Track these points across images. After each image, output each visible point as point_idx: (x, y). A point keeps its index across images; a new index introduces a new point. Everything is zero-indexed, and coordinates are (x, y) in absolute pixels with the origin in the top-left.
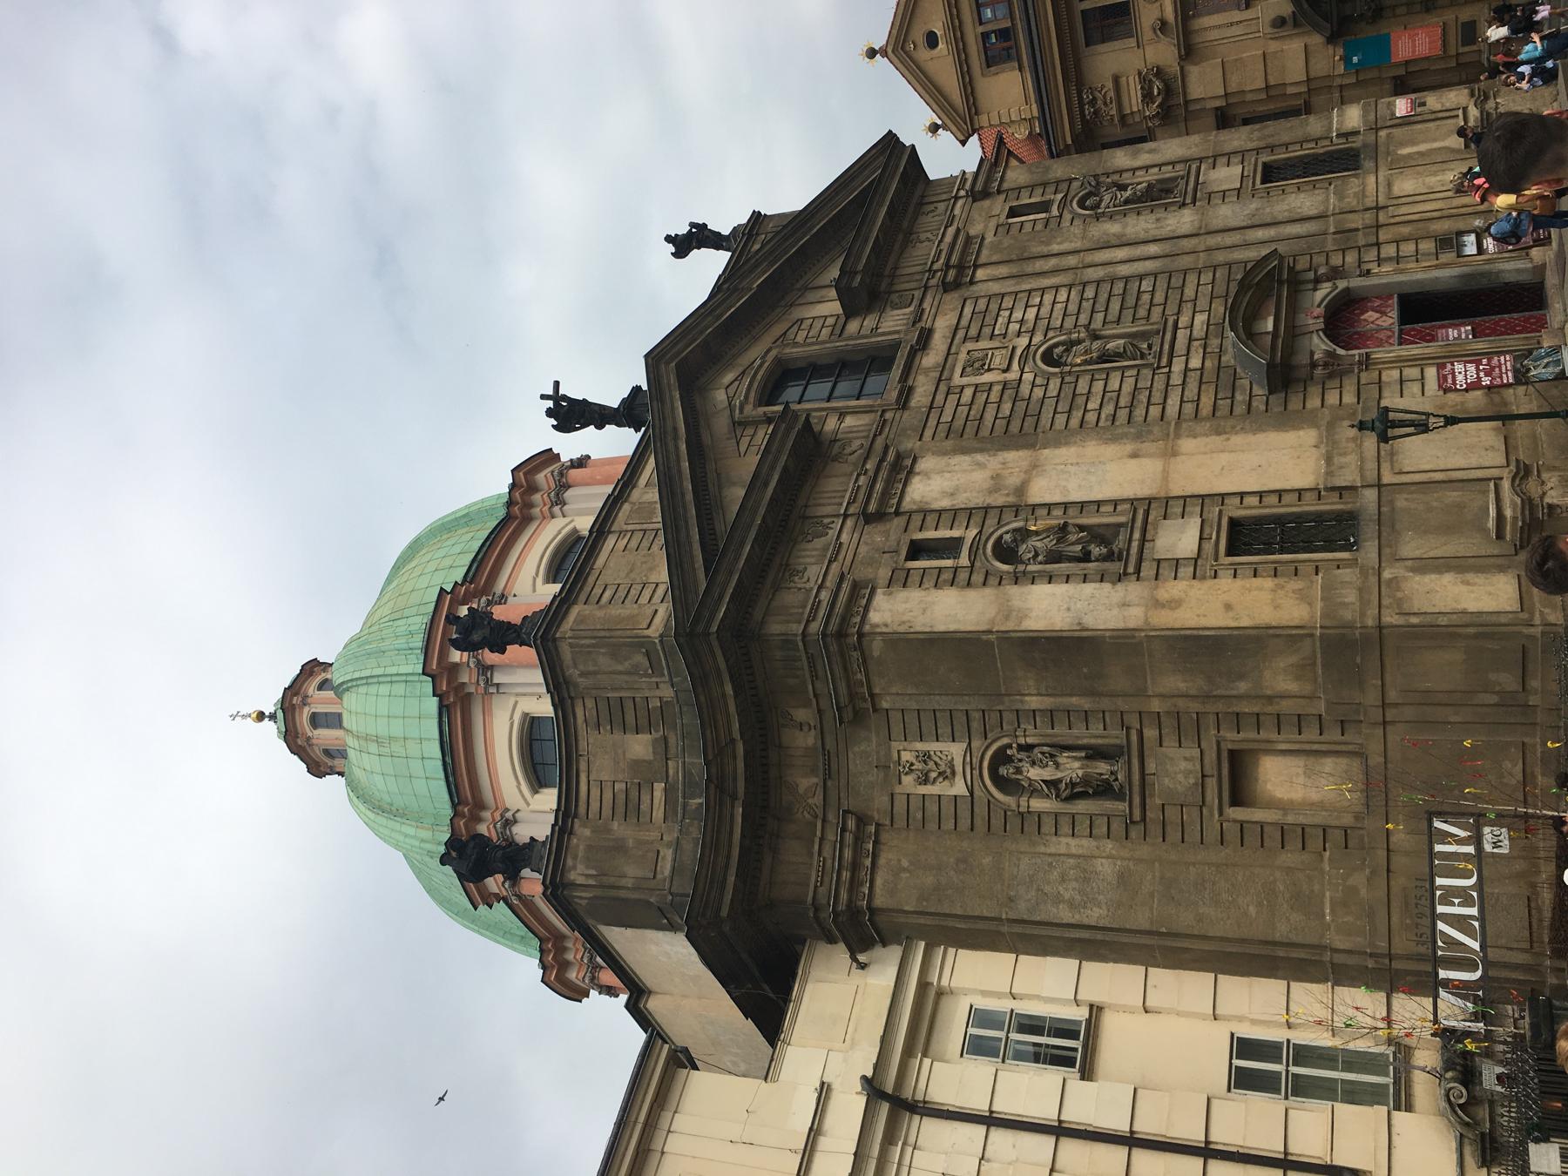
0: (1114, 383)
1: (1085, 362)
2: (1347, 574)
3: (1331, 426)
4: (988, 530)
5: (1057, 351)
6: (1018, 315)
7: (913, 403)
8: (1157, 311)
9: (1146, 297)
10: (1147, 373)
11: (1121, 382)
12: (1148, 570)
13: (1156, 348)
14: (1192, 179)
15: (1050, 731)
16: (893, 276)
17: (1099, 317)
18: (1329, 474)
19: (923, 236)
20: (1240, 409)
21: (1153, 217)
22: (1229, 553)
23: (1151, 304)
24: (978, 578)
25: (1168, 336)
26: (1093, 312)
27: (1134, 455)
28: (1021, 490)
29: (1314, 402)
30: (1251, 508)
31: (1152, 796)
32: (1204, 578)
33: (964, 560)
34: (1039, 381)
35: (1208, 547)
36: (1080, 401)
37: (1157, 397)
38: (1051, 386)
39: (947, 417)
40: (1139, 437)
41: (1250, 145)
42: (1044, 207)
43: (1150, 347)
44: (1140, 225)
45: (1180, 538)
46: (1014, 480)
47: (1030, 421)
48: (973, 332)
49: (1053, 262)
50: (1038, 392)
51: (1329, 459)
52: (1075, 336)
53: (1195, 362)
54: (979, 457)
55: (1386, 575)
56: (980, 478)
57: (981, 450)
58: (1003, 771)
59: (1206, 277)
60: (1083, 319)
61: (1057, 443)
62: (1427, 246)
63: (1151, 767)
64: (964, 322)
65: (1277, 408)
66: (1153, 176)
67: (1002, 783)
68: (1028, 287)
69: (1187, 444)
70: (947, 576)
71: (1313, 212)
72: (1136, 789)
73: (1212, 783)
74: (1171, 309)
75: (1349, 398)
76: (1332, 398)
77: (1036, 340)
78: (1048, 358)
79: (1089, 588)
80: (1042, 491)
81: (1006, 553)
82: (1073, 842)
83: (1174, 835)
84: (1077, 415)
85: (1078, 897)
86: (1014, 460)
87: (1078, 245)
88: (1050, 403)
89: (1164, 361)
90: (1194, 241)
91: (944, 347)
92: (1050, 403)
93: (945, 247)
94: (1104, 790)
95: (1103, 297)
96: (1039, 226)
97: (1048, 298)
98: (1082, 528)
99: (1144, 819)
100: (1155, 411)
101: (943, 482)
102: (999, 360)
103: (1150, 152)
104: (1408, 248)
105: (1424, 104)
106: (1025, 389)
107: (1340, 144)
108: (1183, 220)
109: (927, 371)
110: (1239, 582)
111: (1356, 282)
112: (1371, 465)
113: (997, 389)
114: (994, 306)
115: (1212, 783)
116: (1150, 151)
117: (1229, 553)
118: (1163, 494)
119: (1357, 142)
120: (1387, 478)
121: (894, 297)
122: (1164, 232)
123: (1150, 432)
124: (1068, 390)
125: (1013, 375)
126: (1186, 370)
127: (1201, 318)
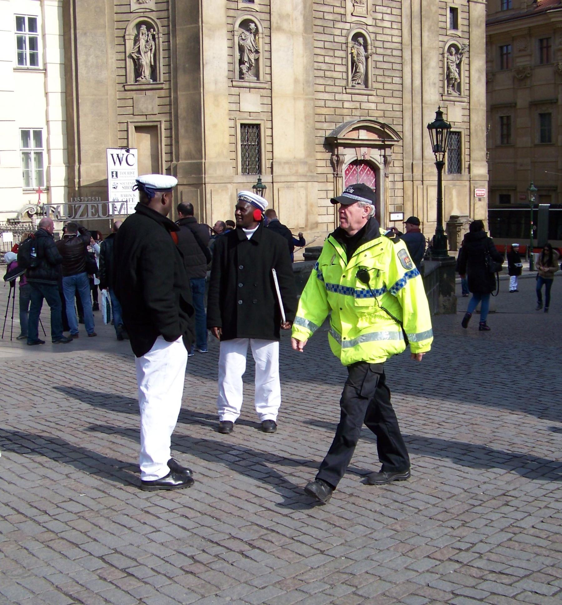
0: (338, 68)
1: (352, 53)
2: (231, 171)
3: (305, 163)
4: (259, 16)
5: (361, 40)
6: (386, 17)
8: (380, 86)
9: (389, 80)
10: (344, 83)
11: (341, 71)
12: (235, 91)
13: (357, 86)
14: (458, 99)
15: (161, 49)
17: (381, 58)
18: (280, 163)
20: (318, 125)
21: (437, 81)
22: (242, 125)
24: (232, 13)
25: (365, 92)
26: (384, 55)
27: (296, 81)
28: (279, 29)
29: (319, 156)
30: (265, 132)
31: (137, 94)
32: (229, 115)
35: (246, 115)
36: (331, 53)
37: (328, 89)
38: (340, 38)
40: (307, 82)
42: (455, 26)
43: (358, 84)
44: (434, 75)
45: (251, 103)
46: (285, 25)
47: (321, 29)
49: (416, 32)
50: (338, 32)
51: (287, 163)
52: (369, 47)
54: (300, 7)
55: (229, 185)
56: (288, 8)
57: (305, 7)
58: (144, 28)
59: (396, 108)
60: (379, 51)
61: (306, 44)
62: (399, 201)
63: (148, 93)
65: (317, 141)
66: (464, 80)
67: (138, 26)
69: (300, 104)
72: (139, 87)
73: (143, 119)
74: (380, 92)
75: (320, 170)
76: (323, 163)
77: (371, 29)
78: (357, 36)
79: (225, 67)
80: (278, 39)
81: (245, 24)
82: (114, 60)
83: (122, 103)
84: (322, 52)
85: (90, 64)
86: (298, 23)
88: (331, 38)
89: (348, 91)
92: (331, 38)
94: (138, 73)
96: (442, 25)
98: (257, 60)
99: (125, 90)
100: (321, 88)
103: (479, 77)
104: (399, 193)
105: (480, 200)
106: (340, 25)
107: (465, 165)
110: (227, 129)
111: (382, 173)
112: (283, 179)
113: (342, 11)
114: (394, 4)
115: (143, 119)
116: (479, 80)
117: (242, 125)
119: (465, 172)
122: (426, 87)
123: (309, 86)
124: (338, 46)
125: (349, 18)
126: (343, 101)
127: (373, 106)
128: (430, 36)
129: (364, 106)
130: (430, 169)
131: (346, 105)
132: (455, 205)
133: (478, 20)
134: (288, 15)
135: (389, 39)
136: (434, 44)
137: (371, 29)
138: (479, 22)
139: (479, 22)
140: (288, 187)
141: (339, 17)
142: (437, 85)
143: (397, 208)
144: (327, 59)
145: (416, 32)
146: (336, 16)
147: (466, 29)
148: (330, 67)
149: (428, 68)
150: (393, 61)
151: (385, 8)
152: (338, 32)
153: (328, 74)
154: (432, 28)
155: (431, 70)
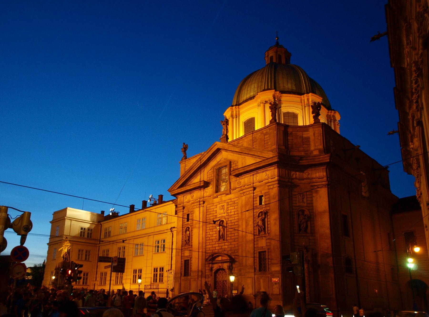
6: (232, 211)
7: (214, 199)
8: (230, 238)
19: (258, 178)
23: (231, 237)
28: (195, 227)
36: (212, 231)
45: (187, 253)
48: (230, 203)
59: (236, 245)
64: (232, 200)
105: (276, 284)
108: (250, 237)
109: (221, 199)
113: (216, 214)
114: (236, 204)
116: (275, 224)
117: (185, 261)
120: (192, 280)
121: (241, 181)
125: (218, 216)
126: (215, 247)
127: (226, 247)
129: (223, 247)
131: (217, 248)
135: (233, 218)
140: (194, 280)
144: (211, 233)
153: (211, 238)
155: (249, 226)
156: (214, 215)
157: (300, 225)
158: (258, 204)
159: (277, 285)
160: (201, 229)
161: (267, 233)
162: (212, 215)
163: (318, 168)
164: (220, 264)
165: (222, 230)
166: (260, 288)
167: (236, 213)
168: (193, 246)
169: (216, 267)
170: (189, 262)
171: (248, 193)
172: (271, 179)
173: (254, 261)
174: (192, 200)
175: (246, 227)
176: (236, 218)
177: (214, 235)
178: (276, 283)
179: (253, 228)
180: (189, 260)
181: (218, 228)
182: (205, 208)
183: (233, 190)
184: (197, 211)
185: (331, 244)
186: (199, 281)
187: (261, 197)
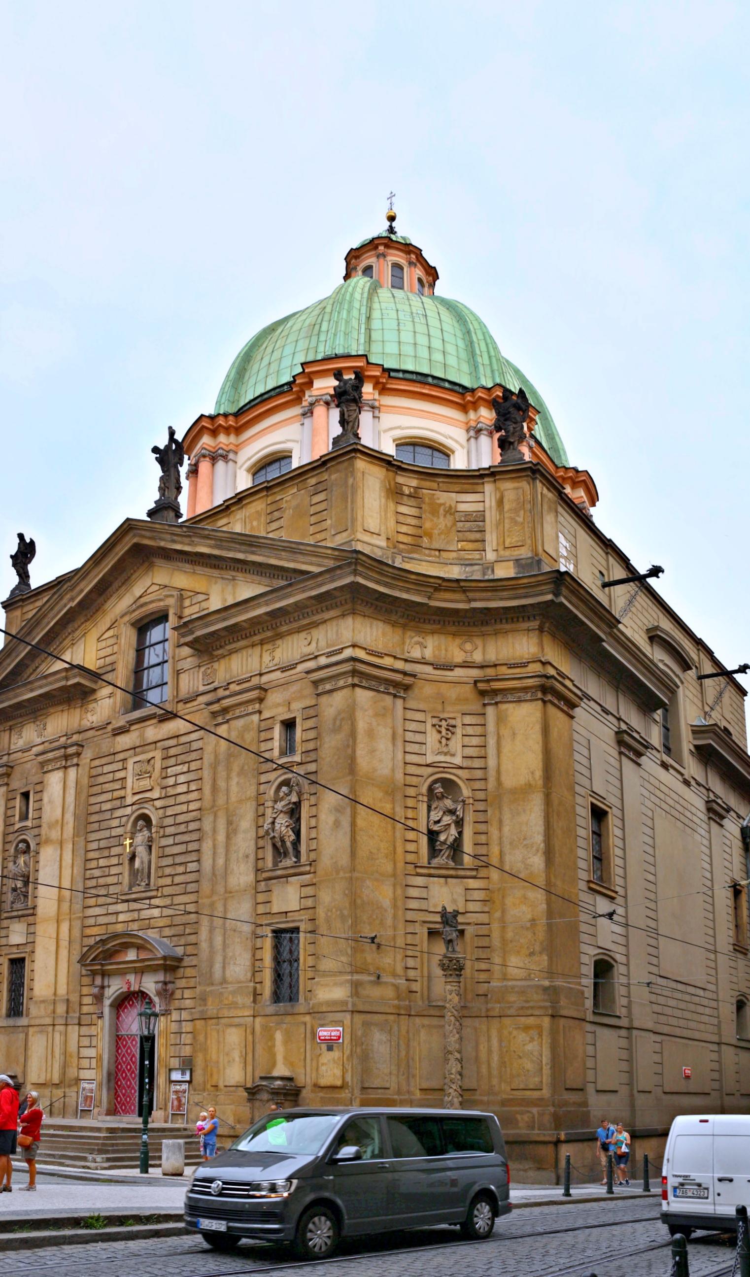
6: (182, 779)
8: (168, 881)
14: (292, 871)
16: (231, 653)
18: (36, 1002)
19: (278, 654)
23: (173, 876)
28: (48, 841)
33: (17, 826)
34: (124, 819)
39: (106, 769)
41: (321, 913)
48: (172, 752)
53: (122, 917)
62: (187, 1051)
68: (206, 774)
69: (65, 927)
70: (12, 820)
71: (228, 973)
75: (85, 1009)
77: (158, 804)
87: (233, 798)
88: (106, 834)
90: (222, 890)
91: (160, 737)
92: (106, 834)
93: (255, 681)
95: (186, 838)
97: (194, 796)
101: (58, 792)
102: (145, 783)
104: (187, 1039)
108: (242, 875)
109: (142, 736)
114: (194, 756)
116: (337, 824)
118: (38, 920)
119: (301, 999)
122: (233, 866)
125: (129, 800)
128: (242, 781)
130: (230, 998)
132: (280, 1058)
133: (335, 720)
134: (57, 821)
135: (184, 808)
136: (248, 793)
137: (158, 804)
138: (338, 723)
139: (338, 723)
141: (117, 803)
142: (252, 858)
143: (183, 1062)
145: (222, 784)
146: (115, 802)
147: (311, 746)
148: (104, 872)
149: (235, 834)
150: (188, 839)
151: (181, 766)
152: (115, 823)
154: (246, 767)
156: (117, 794)
157: (432, 836)
158: (276, 753)
159: (336, 1054)
160: (68, 847)
161: (303, 859)
162: (108, 796)
163: (508, 627)
164: (131, 978)
165: (141, 851)
166: (274, 1065)
167: (193, 787)
168: (40, 911)
169: (115, 987)
170: (23, 967)
171: (238, 712)
172: (329, 655)
173: (253, 965)
174: (39, 740)
175: (228, 837)
176: (192, 806)
177: (114, 871)
178: (330, 1044)
179: (253, 843)
180: (23, 960)
181: (128, 842)
182: (84, 770)
183: (186, 701)
184: (54, 780)
185: (544, 906)
186: (57, 1036)
187: (289, 725)
